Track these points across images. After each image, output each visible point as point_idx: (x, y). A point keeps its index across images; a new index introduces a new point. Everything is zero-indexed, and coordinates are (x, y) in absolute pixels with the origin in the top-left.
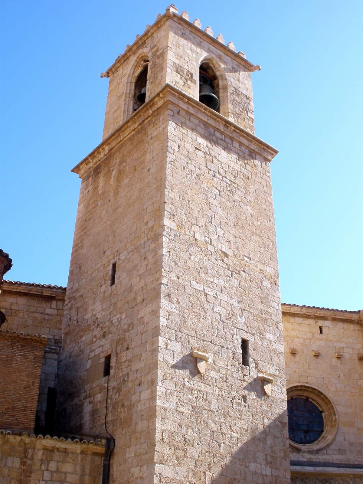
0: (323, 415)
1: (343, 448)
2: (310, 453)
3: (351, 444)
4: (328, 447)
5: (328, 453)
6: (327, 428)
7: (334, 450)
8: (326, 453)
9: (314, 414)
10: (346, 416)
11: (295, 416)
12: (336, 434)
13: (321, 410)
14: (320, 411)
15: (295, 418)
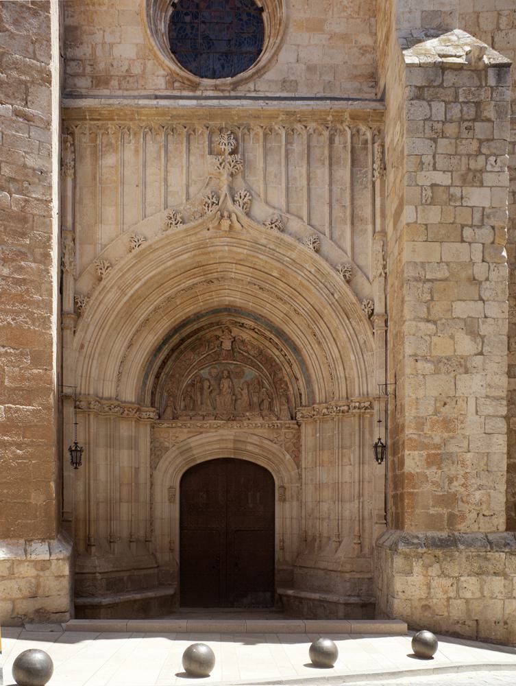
0: (265, 15)
1: (292, 78)
2: (219, 90)
3: (310, 69)
4: (259, 77)
5: (257, 89)
6: (270, 43)
7: (272, 81)
8: (253, 90)
9: (245, 17)
10: (306, 7)
11: (204, 22)
12: (279, 48)
13: (260, 5)
14: (257, 7)
15: (203, 25)
